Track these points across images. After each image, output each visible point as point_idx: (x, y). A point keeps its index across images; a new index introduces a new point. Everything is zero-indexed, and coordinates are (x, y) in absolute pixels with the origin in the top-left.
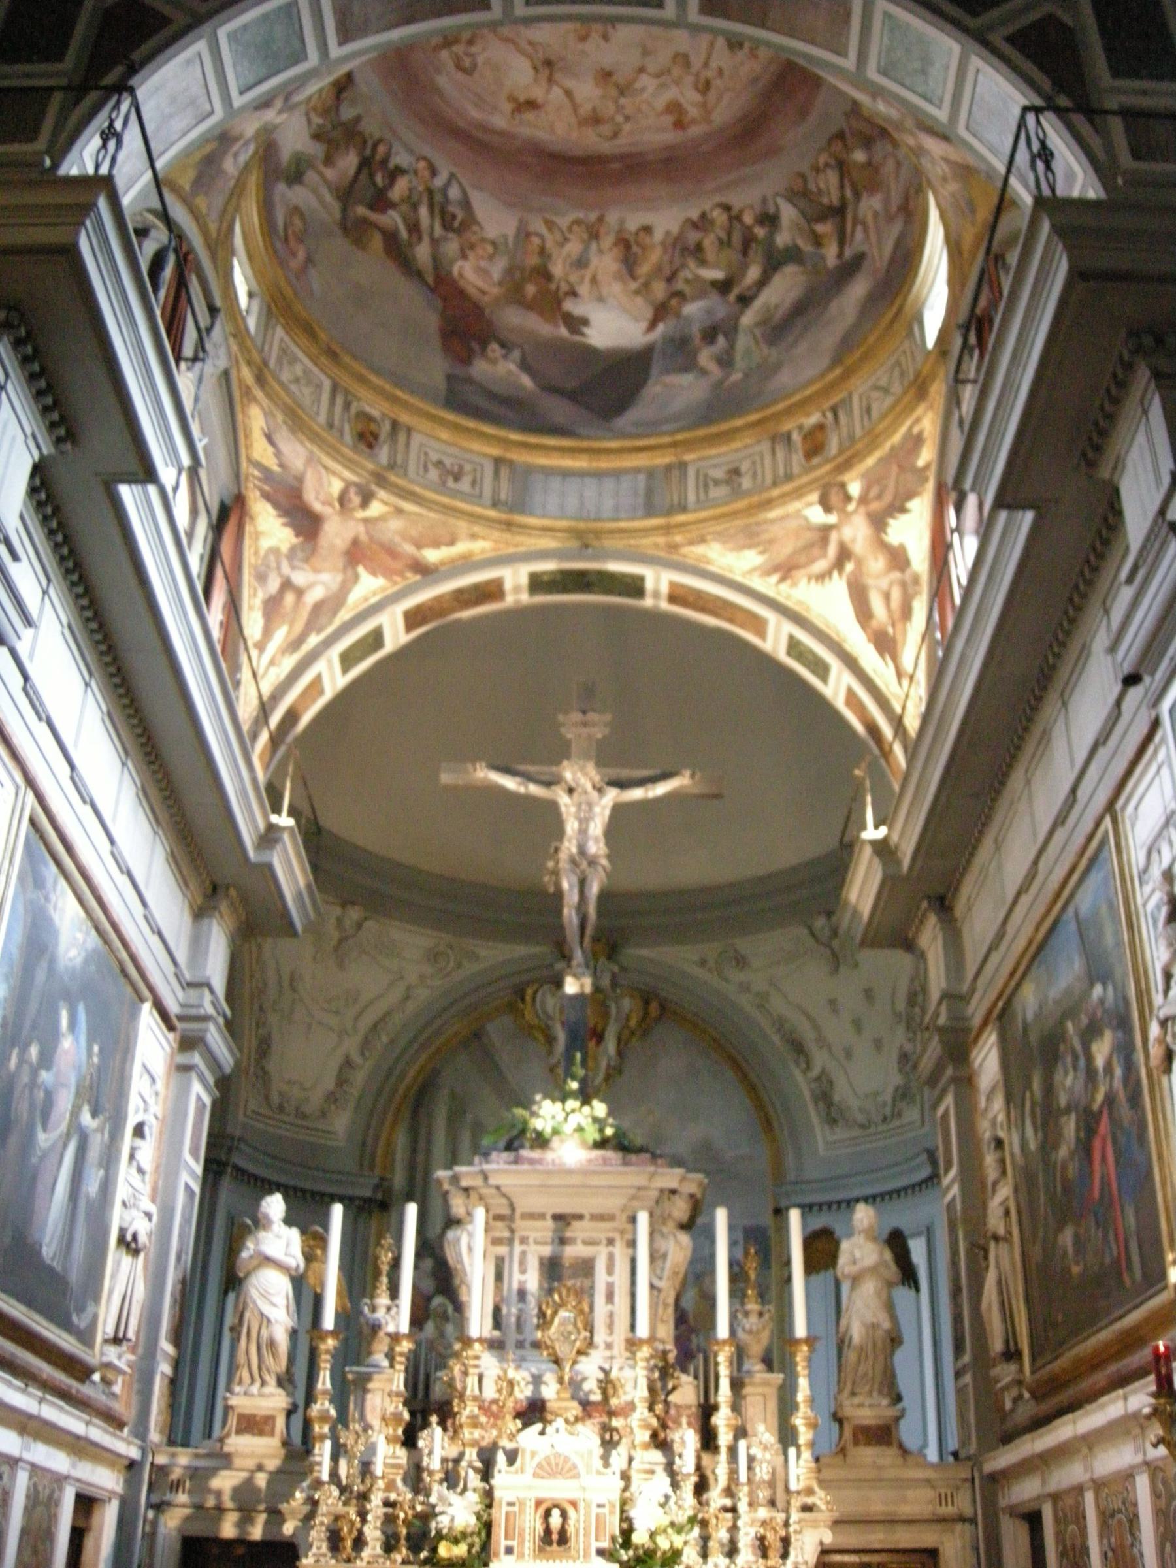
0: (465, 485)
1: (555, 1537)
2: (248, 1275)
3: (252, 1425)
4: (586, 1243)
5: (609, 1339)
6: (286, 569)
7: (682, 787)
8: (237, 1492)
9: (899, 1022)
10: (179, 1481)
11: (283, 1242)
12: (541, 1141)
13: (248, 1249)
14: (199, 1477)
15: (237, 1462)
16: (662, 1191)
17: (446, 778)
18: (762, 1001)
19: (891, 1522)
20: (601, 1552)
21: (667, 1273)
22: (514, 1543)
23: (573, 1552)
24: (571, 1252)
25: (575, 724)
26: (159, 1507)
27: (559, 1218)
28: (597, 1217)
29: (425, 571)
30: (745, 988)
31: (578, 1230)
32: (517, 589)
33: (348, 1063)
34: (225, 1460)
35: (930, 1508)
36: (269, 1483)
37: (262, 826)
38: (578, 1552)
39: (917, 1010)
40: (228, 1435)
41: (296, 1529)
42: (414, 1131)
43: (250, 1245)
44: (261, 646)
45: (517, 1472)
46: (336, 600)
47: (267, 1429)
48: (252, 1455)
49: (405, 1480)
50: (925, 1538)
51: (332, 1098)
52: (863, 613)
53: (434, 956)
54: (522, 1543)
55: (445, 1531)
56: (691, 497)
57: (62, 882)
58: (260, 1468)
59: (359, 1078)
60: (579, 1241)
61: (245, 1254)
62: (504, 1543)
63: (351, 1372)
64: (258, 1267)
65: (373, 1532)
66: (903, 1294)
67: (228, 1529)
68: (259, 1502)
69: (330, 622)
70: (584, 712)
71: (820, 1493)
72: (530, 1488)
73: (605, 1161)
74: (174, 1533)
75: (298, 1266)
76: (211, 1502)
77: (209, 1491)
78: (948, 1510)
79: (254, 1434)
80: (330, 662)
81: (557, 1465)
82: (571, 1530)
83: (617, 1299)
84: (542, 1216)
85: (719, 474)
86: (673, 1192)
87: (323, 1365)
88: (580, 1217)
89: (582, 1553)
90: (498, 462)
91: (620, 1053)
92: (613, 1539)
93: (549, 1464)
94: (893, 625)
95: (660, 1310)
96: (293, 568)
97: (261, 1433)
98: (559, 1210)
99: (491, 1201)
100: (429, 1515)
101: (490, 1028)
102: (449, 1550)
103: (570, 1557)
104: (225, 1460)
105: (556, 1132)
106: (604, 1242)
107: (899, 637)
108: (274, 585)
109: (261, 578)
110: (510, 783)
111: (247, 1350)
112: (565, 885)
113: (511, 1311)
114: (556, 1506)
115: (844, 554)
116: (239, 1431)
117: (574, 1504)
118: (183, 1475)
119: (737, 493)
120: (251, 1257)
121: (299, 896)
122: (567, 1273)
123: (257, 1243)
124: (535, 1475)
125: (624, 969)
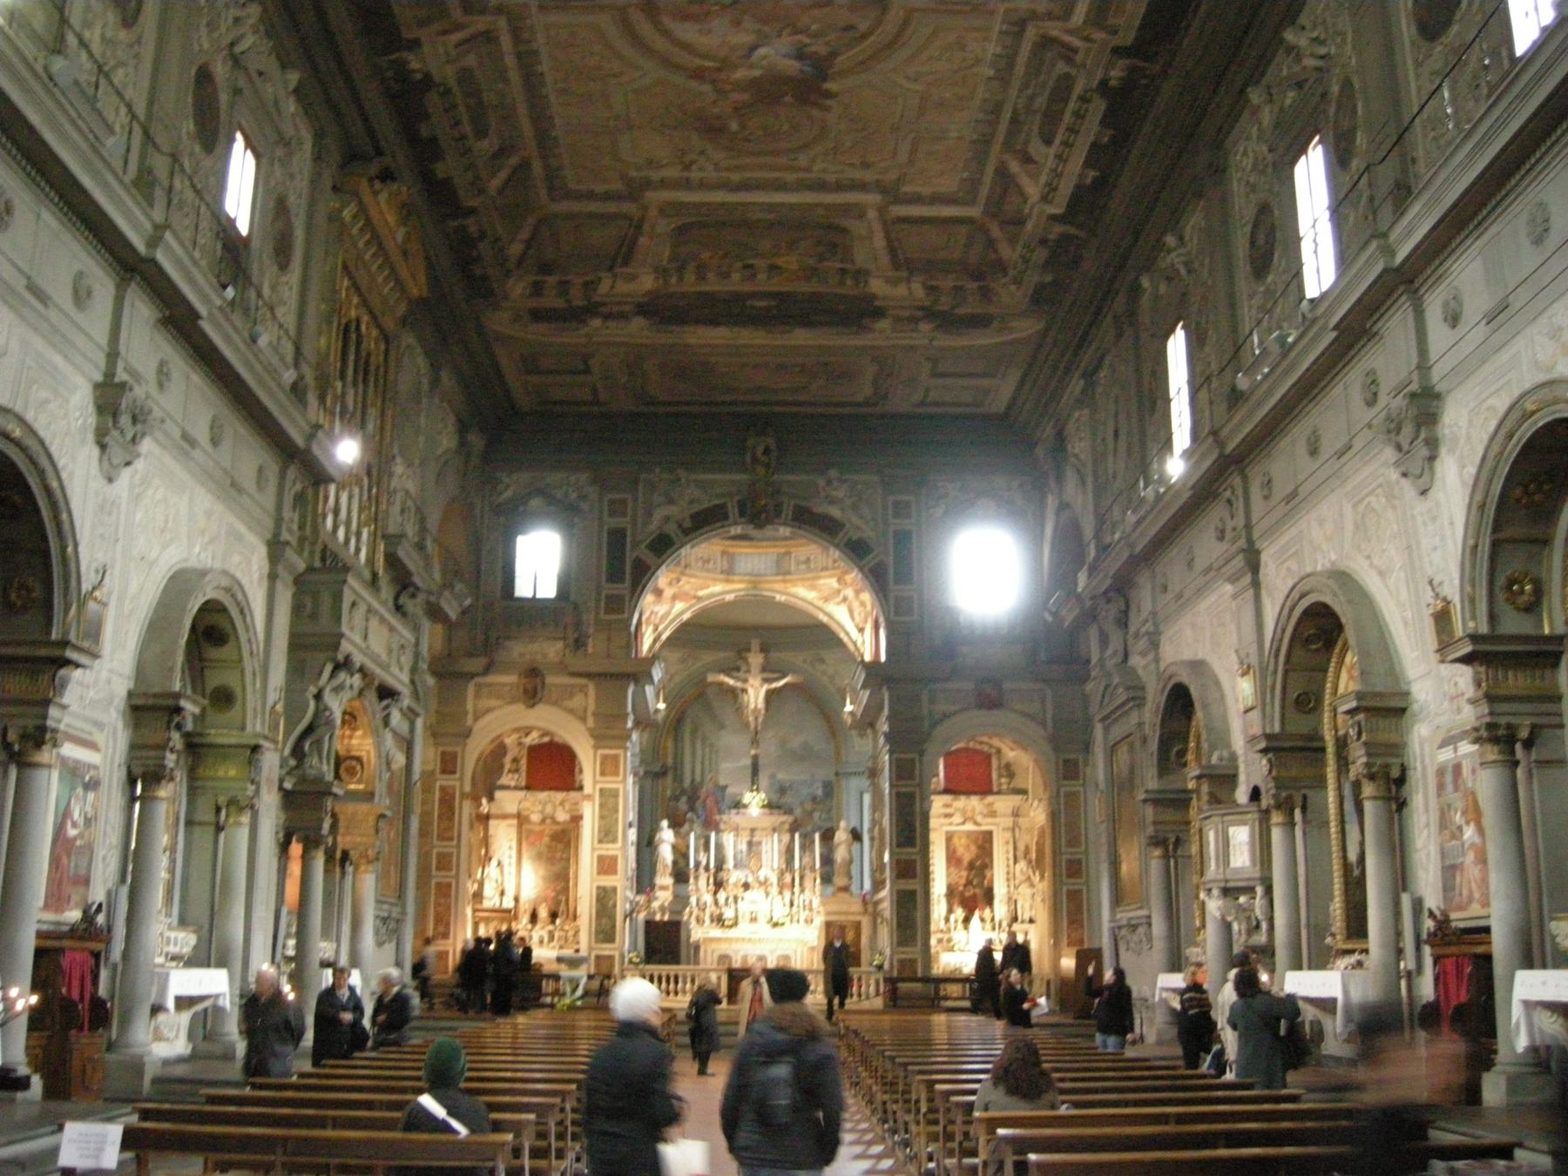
0: (711, 565)
3: (663, 888)
12: (745, 806)
18: (832, 678)
19: (847, 913)
24: (756, 839)
29: (699, 599)
30: (824, 673)
31: (757, 833)
42: (676, 740)
46: (668, 613)
50: (858, 918)
53: (683, 661)
56: (793, 568)
65: (707, 919)
66: (856, 846)
67: (658, 917)
85: (803, 558)
90: (724, 553)
111: (659, 867)
115: (845, 599)
119: (809, 570)
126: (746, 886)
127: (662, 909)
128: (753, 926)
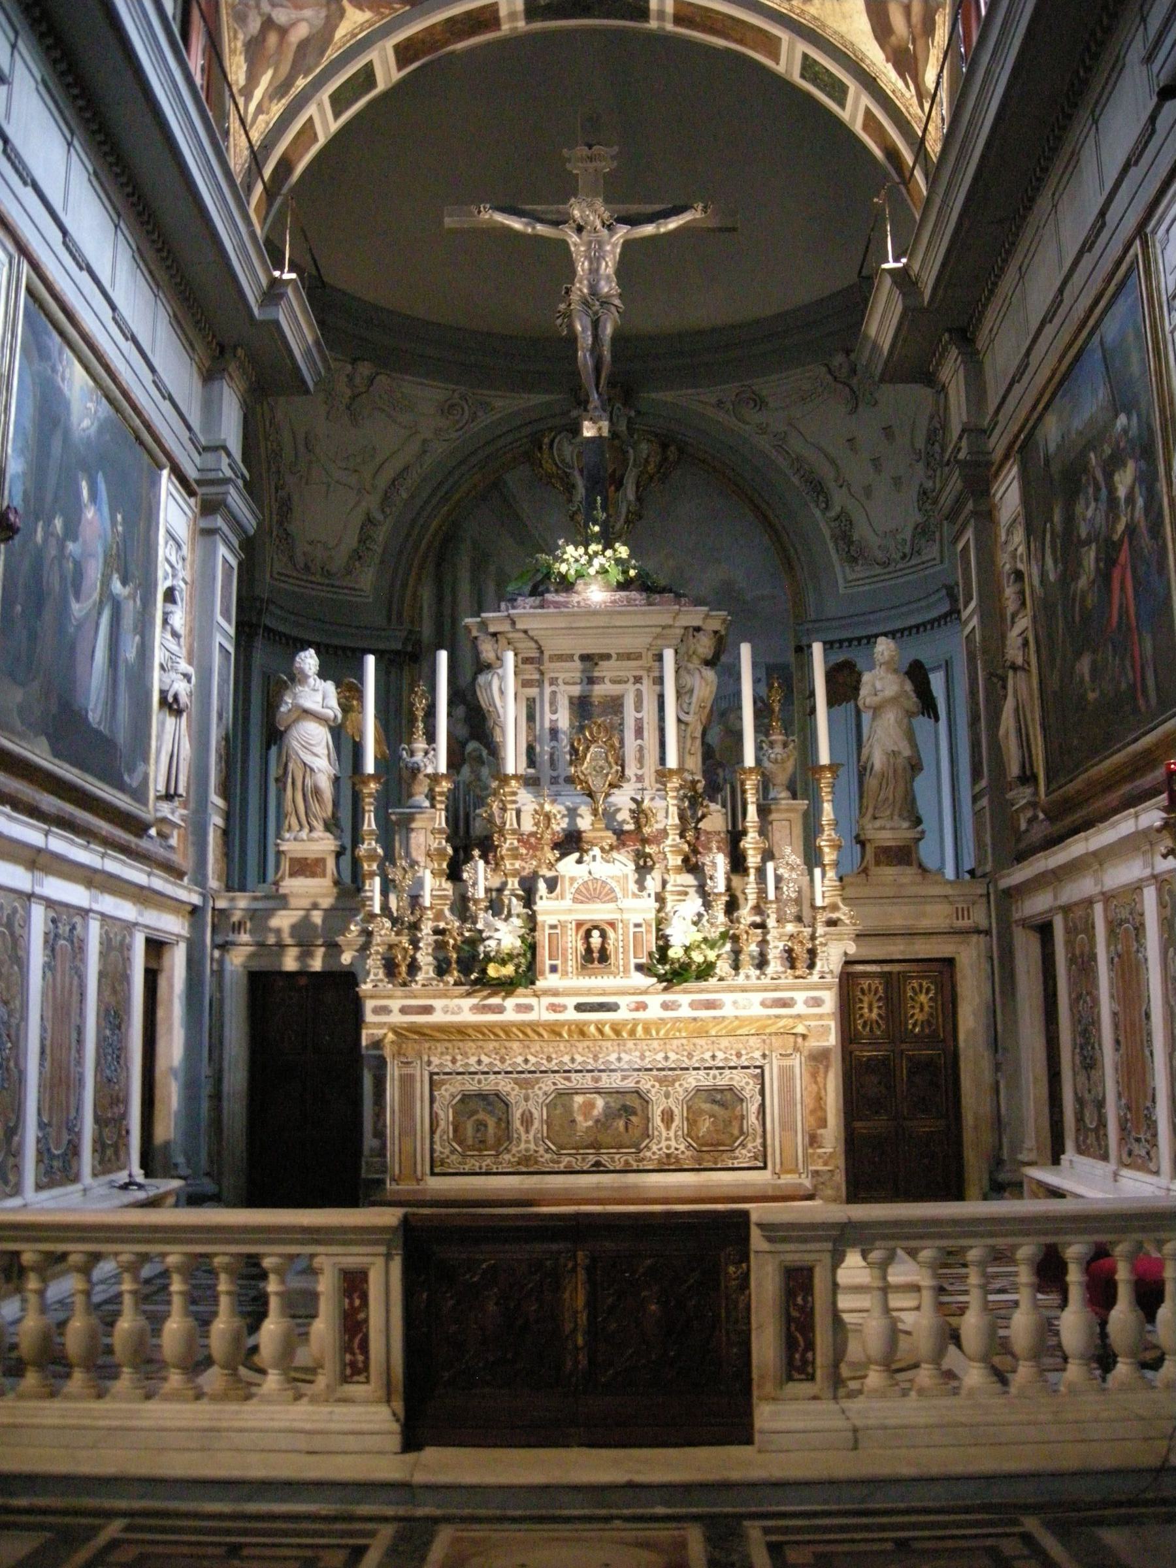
1: (596, 955)
2: (288, 728)
3: (305, 867)
4: (613, 682)
5: (640, 772)
6: (266, 7)
7: (694, 220)
8: (294, 928)
9: (918, 461)
10: (240, 923)
11: (319, 697)
12: (565, 584)
13: (287, 703)
14: (258, 918)
15: (293, 902)
16: (686, 628)
17: (449, 222)
19: (911, 934)
20: (639, 968)
21: (693, 708)
22: (558, 962)
23: (613, 968)
24: (599, 690)
25: (582, 160)
26: (224, 947)
27: (585, 658)
28: (622, 657)
30: (763, 429)
31: (605, 670)
32: (512, 16)
33: (369, 520)
34: (282, 901)
35: (948, 921)
36: (324, 921)
37: (264, 282)
38: (618, 968)
39: (937, 447)
40: (282, 878)
41: (354, 958)
42: (439, 581)
43: (288, 699)
44: (247, 92)
45: (557, 899)
46: (323, 36)
47: (319, 870)
48: (306, 895)
49: (451, 910)
51: (356, 556)
52: (882, 30)
53: (447, 409)
54: (565, 961)
55: (492, 954)
57: (68, 353)
58: (315, 906)
59: (381, 534)
60: (606, 680)
61: (283, 709)
62: (548, 963)
63: (394, 813)
64: (297, 720)
65: (425, 958)
66: (923, 724)
67: (290, 963)
68: (317, 937)
69: (317, 65)
70: (590, 147)
71: (845, 909)
72: (570, 911)
73: (629, 600)
74: (240, 969)
75: (336, 716)
76: (271, 940)
77: (271, 930)
78: (961, 924)
79: (307, 877)
80: (320, 105)
81: (595, 889)
82: (610, 948)
83: (646, 734)
84: (570, 658)
86: (698, 629)
87: (367, 808)
88: (607, 657)
89: (621, 969)
91: (639, 499)
92: (650, 954)
93: (588, 889)
94: (914, 43)
95: (689, 742)
96: (273, 5)
97: (313, 875)
98: (585, 652)
99: (519, 645)
100: (478, 939)
101: (508, 477)
102: (498, 971)
103: (611, 973)
104: (282, 901)
105: (580, 575)
106: (632, 680)
107: (920, 56)
108: (255, 25)
109: (241, 18)
110: (517, 224)
111: (294, 798)
112: (579, 327)
113: (544, 750)
114: (596, 927)
116: (292, 874)
117: (612, 924)
118: (243, 917)
120: (290, 711)
121: (308, 353)
122: (596, 711)
123: (295, 696)
124: (575, 900)
125: (638, 413)
126: (571, 842)
127: (304, 936)
128: (599, 983)
